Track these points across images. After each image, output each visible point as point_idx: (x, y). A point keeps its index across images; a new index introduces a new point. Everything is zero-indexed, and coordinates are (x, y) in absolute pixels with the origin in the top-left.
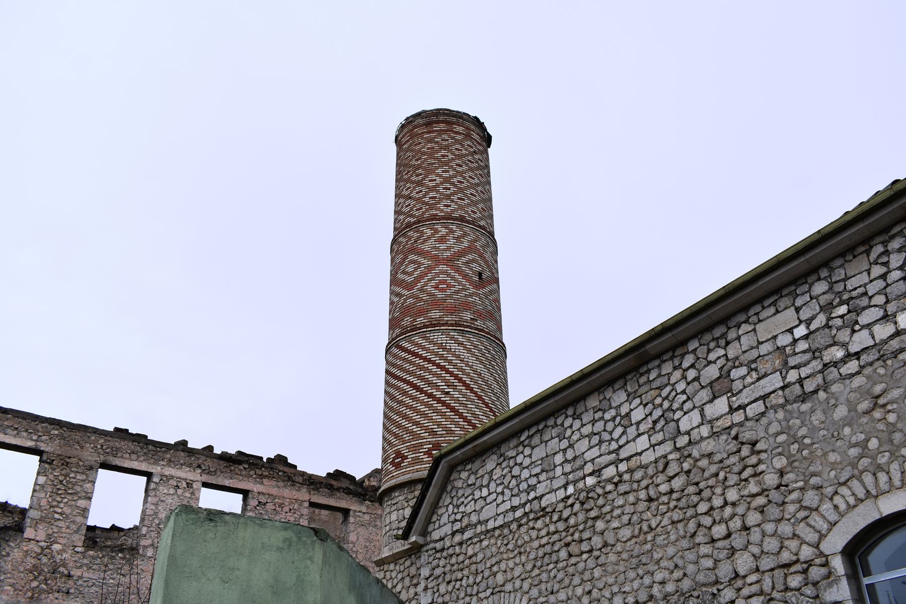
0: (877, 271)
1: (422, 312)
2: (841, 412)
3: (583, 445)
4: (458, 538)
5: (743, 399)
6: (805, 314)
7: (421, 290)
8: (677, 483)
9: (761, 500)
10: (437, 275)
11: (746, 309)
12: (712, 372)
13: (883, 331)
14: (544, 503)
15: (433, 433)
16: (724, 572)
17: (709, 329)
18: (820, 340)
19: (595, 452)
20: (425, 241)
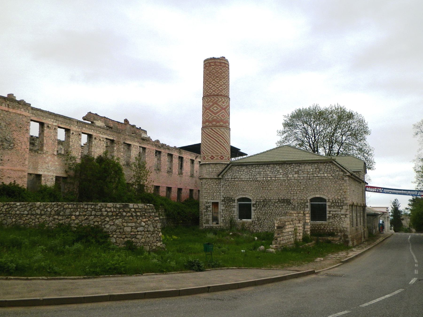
0: (324, 167)
1: (219, 122)
2: (314, 183)
3: (269, 172)
4: (233, 179)
5: (300, 176)
6: (313, 168)
7: (218, 116)
8: (286, 184)
9: (300, 190)
10: (222, 113)
11: (304, 163)
12: (296, 170)
13: (322, 175)
14: (258, 179)
15: (221, 153)
16: (292, 198)
17: (297, 163)
18: (314, 173)
19: (271, 174)
20: (219, 102)
